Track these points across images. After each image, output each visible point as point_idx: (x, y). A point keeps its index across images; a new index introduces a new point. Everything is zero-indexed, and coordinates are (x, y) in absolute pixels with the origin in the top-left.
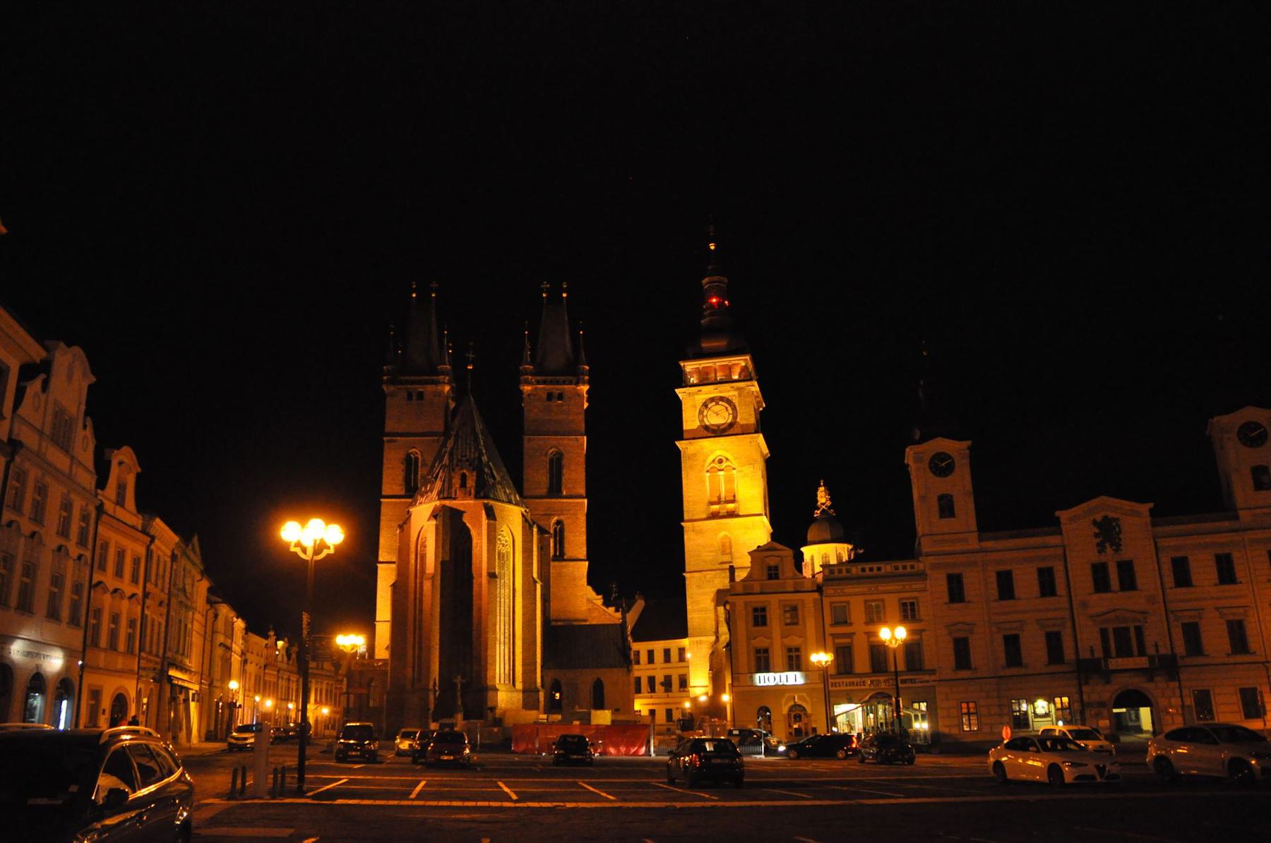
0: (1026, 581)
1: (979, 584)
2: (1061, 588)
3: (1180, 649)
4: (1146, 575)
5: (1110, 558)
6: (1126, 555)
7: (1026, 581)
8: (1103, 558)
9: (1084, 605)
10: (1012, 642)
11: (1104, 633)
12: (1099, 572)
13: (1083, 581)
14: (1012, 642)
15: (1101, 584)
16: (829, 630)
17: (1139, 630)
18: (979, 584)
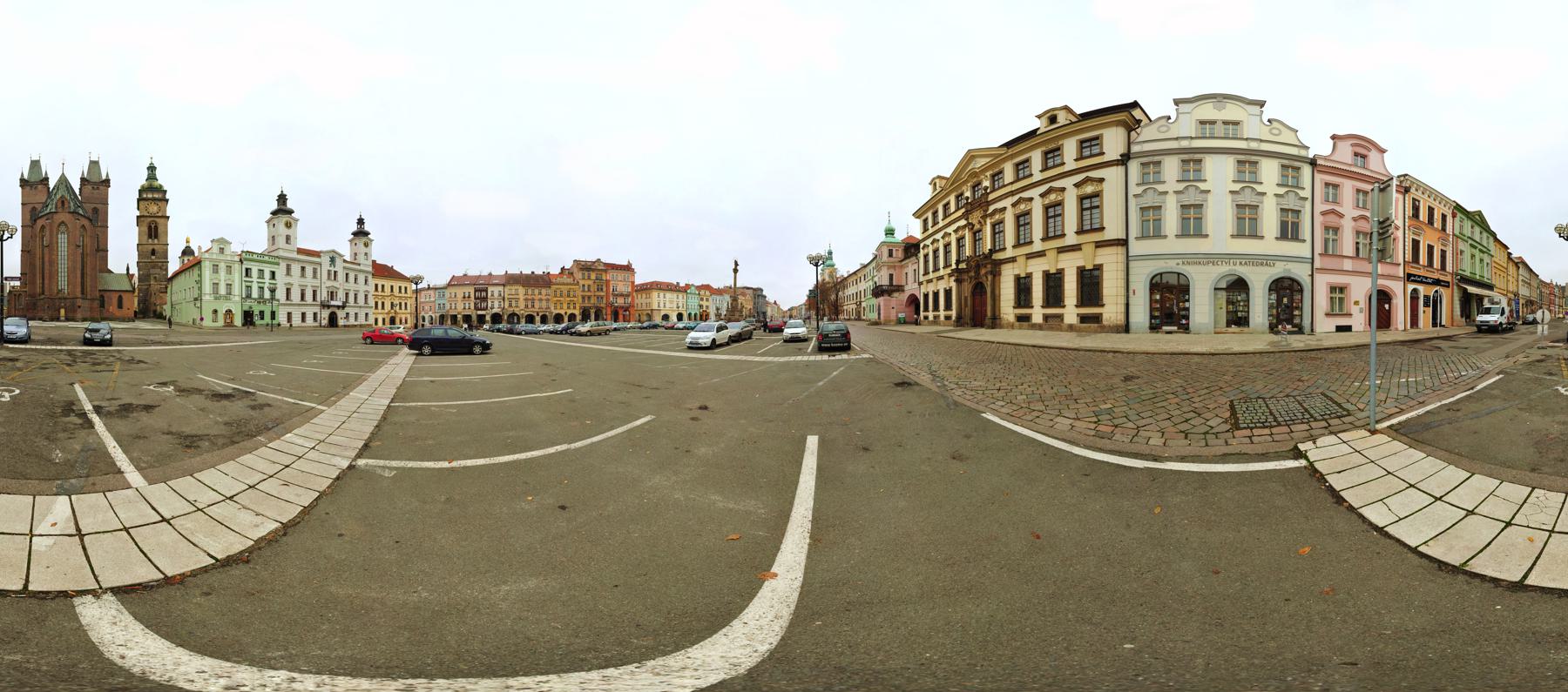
4: (341, 276)
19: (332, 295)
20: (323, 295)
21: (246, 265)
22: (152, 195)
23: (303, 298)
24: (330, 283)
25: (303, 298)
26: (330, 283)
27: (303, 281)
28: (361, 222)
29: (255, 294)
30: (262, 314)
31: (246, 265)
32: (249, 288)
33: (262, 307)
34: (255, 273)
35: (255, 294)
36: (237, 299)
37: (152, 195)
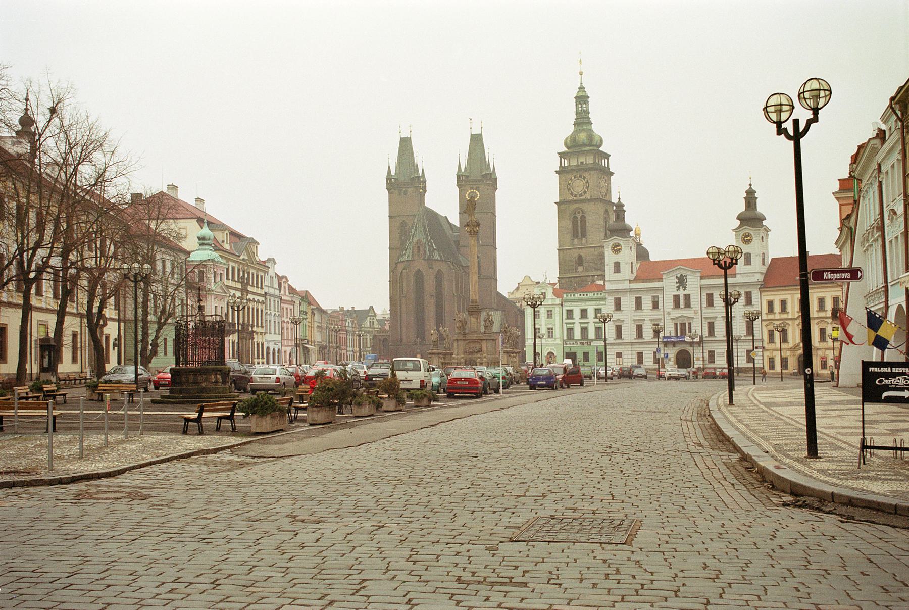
0: (647, 302)
1: (628, 302)
2: (660, 306)
3: (706, 333)
5: (682, 293)
6: (686, 292)
7: (647, 302)
8: (677, 293)
9: (669, 313)
10: (640, 329)
11: (676, 324)
12: (676, 298)
13: (670, 303)
14: (640, 329)
15: (677, 305)
16: (565, 321)
17: (690, 324)
18: (628, 302)
19: (683, 328)
20: (669, 330)
21: (567, 306)
22: (584, 160)
23: (640, 334)
24: (676, 313)
25: (640, 334)
26: (676, 313)
27: (639, 315)
28: (751, 198)
29: (577, 335)
30: (586, 356)
31: (567, 306)
32: (570, 331)
33: (586, 349)
34: (577, 314)
35: (577, 335)
36: (558, 341)
37: (584, 160)
